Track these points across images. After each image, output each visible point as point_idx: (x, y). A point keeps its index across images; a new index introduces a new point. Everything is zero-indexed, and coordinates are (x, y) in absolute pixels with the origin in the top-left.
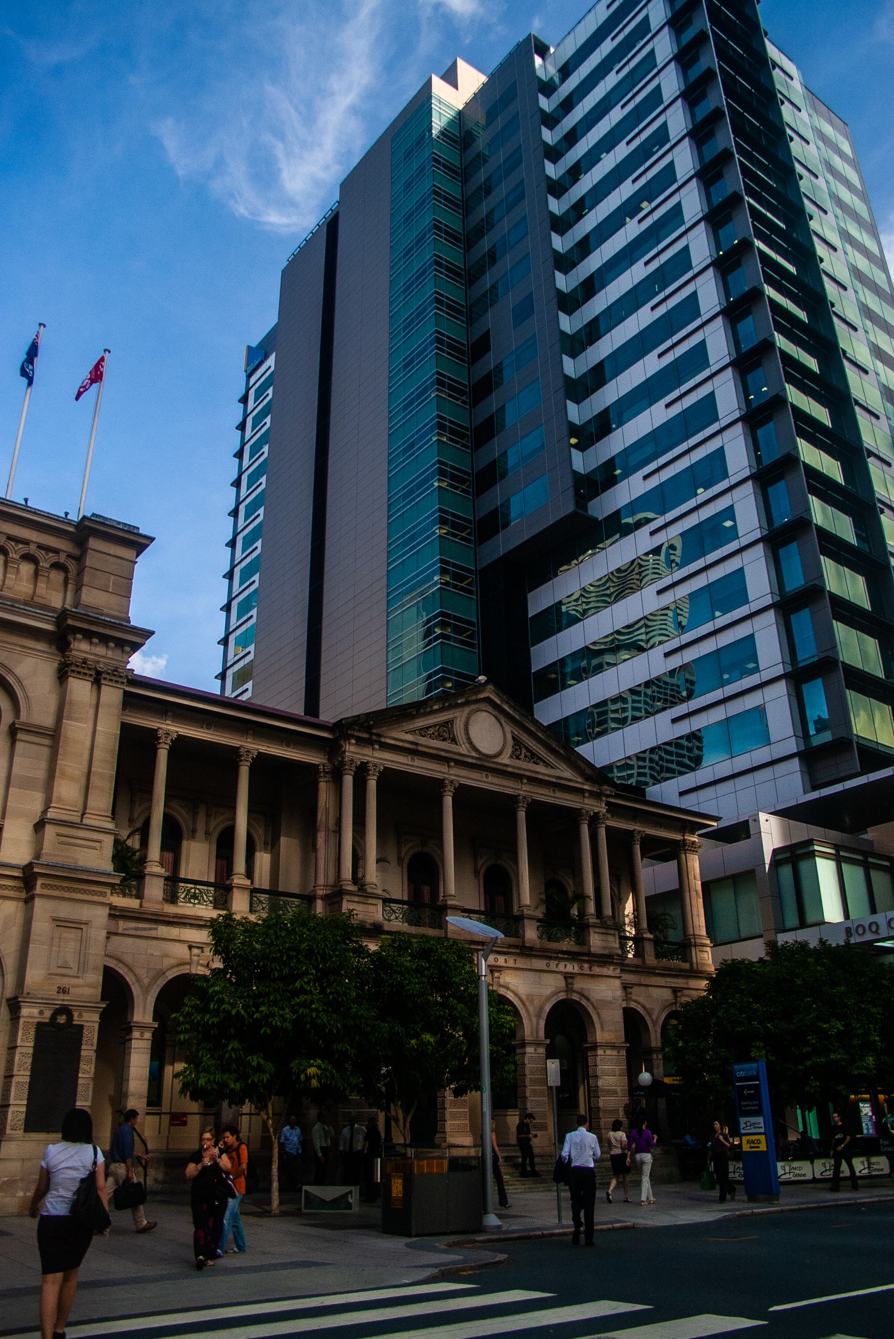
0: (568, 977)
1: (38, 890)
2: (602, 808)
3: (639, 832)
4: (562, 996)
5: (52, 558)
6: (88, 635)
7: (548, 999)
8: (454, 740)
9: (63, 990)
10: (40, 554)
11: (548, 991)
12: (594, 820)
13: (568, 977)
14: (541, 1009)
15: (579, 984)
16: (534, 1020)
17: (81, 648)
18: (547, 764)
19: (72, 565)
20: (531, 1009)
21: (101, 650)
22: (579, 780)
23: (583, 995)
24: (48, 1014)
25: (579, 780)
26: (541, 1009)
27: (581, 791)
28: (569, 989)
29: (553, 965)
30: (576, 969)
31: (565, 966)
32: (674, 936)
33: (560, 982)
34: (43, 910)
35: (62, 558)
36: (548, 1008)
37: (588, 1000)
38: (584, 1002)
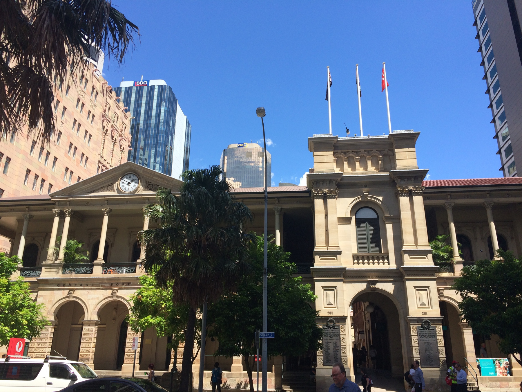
9: (425, 314)
32: (412, 382)
34: (410, 286)
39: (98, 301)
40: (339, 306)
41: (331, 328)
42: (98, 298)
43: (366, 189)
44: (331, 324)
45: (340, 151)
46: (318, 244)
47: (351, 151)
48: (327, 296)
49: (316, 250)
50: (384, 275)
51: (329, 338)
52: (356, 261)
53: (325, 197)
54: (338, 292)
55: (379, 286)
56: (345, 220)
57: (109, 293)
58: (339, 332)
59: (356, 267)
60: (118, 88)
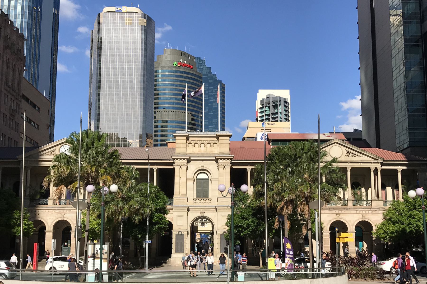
1: (218, 211)
2: (378, 166)
5: (213, 142)
6: (221, 159)
7: (356, 221)
10: (211, 142)
11: (356, 219)
14: (354, 223)
16: (351, 226)
17: (220, 161)
18: (359, 156)
19: (217, 142)
21: (224, 161)
24: (222, 232)
26: (354, 223)
29: (358, 211)
35: (215, 142)
39: (53, 220)
42: (53, 219)
44: (180, 233)
49: (174, 196)
50: (208, 208)
57: (59, 215)
59: (195, 205)
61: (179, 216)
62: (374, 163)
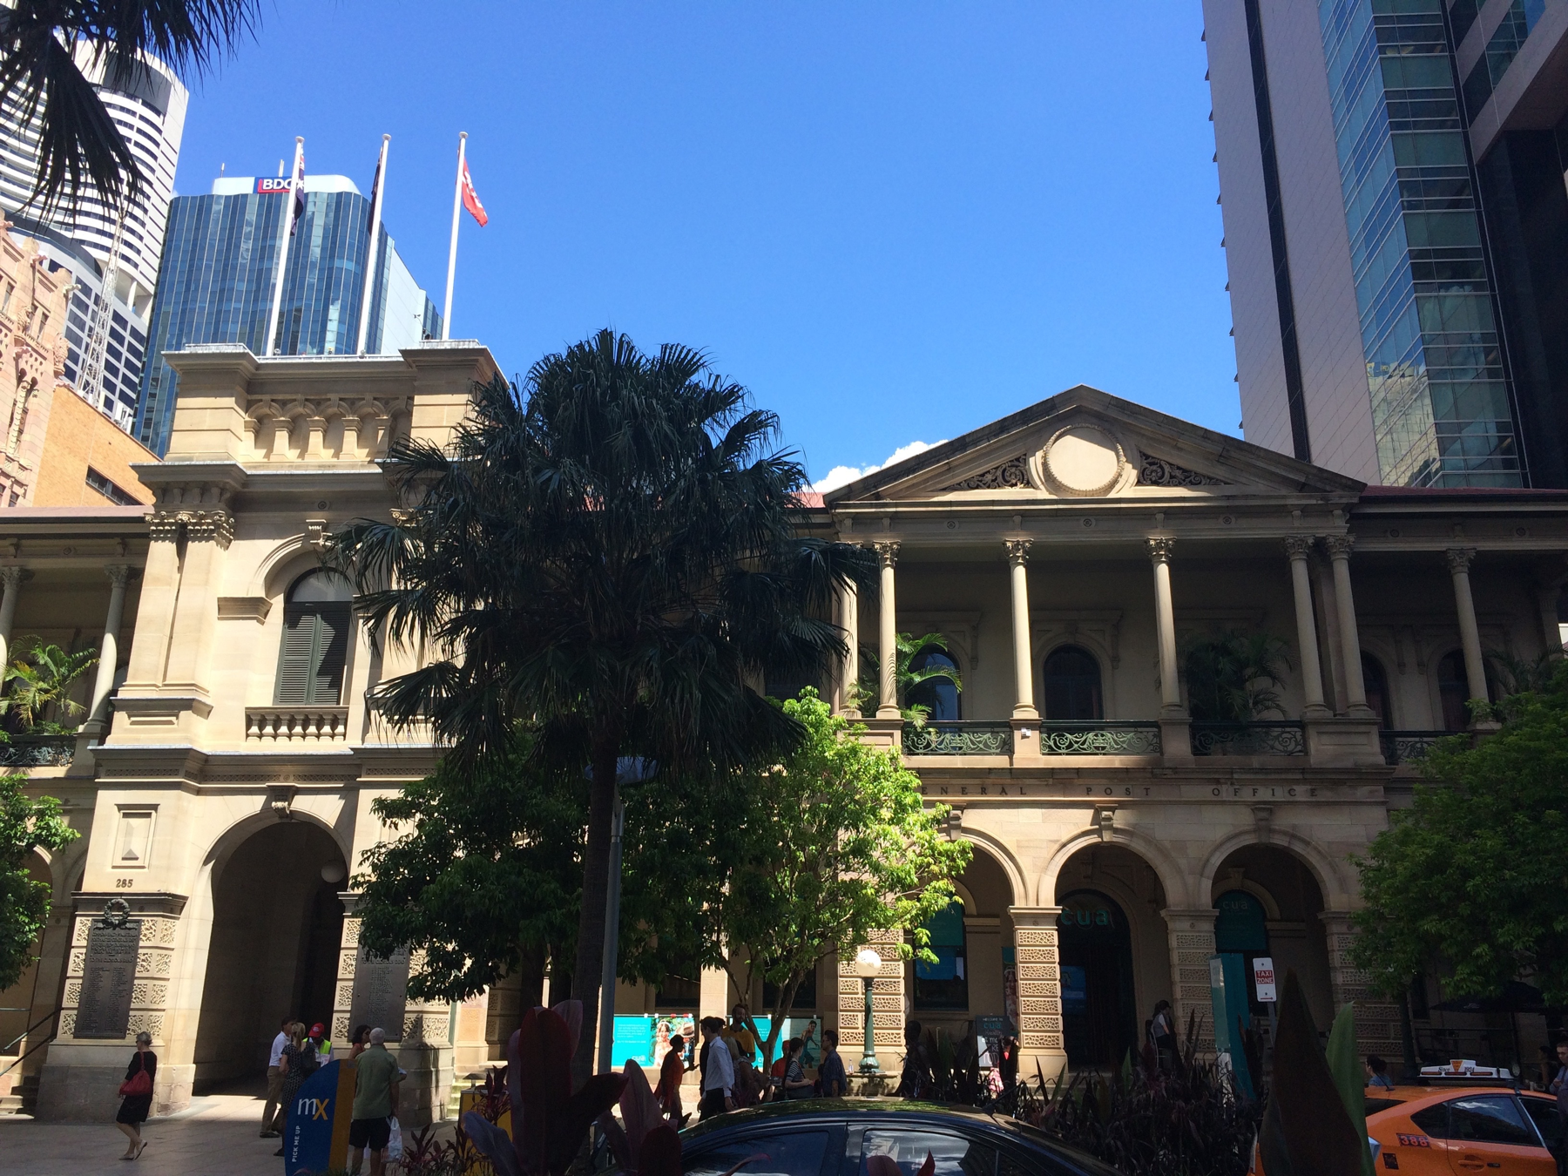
0: (1266, 810)
2: (1336, 528)
3: (1462, 552)
4: (1249, 840)
8: (1029, 483)
11: (1220, 833)
12: (1319, 554)
13: (1266, 810)
15: (1286, 820)
20: (1183, 862)
22: (1284, 492)
23: (1293, 836)
25: (1284, 492)
27: (1282, 511)
28: (1263, 826)
29: (1226, 792)
30: (1280, 795)
31: (1255, 792)
33: (1245, 818)
36: (1217, 860)
37: (1308, 843)
38: (1298, 848)
40: (154, 862)
41: (115, 926)
43: (321, 514)
45: (267, 397)
46: (134, 678)
47: (299, 397)
48: (129, 832)
50: (321, 771)
51: (104, 956)
52: (254, 729)
53: (182, 537)
54: (160, 820)
55: (302, 804)
56: (251, 608)
58: (137, 939)
60: (202, 198)
61: (129, 811)
62: (1306, 511)
